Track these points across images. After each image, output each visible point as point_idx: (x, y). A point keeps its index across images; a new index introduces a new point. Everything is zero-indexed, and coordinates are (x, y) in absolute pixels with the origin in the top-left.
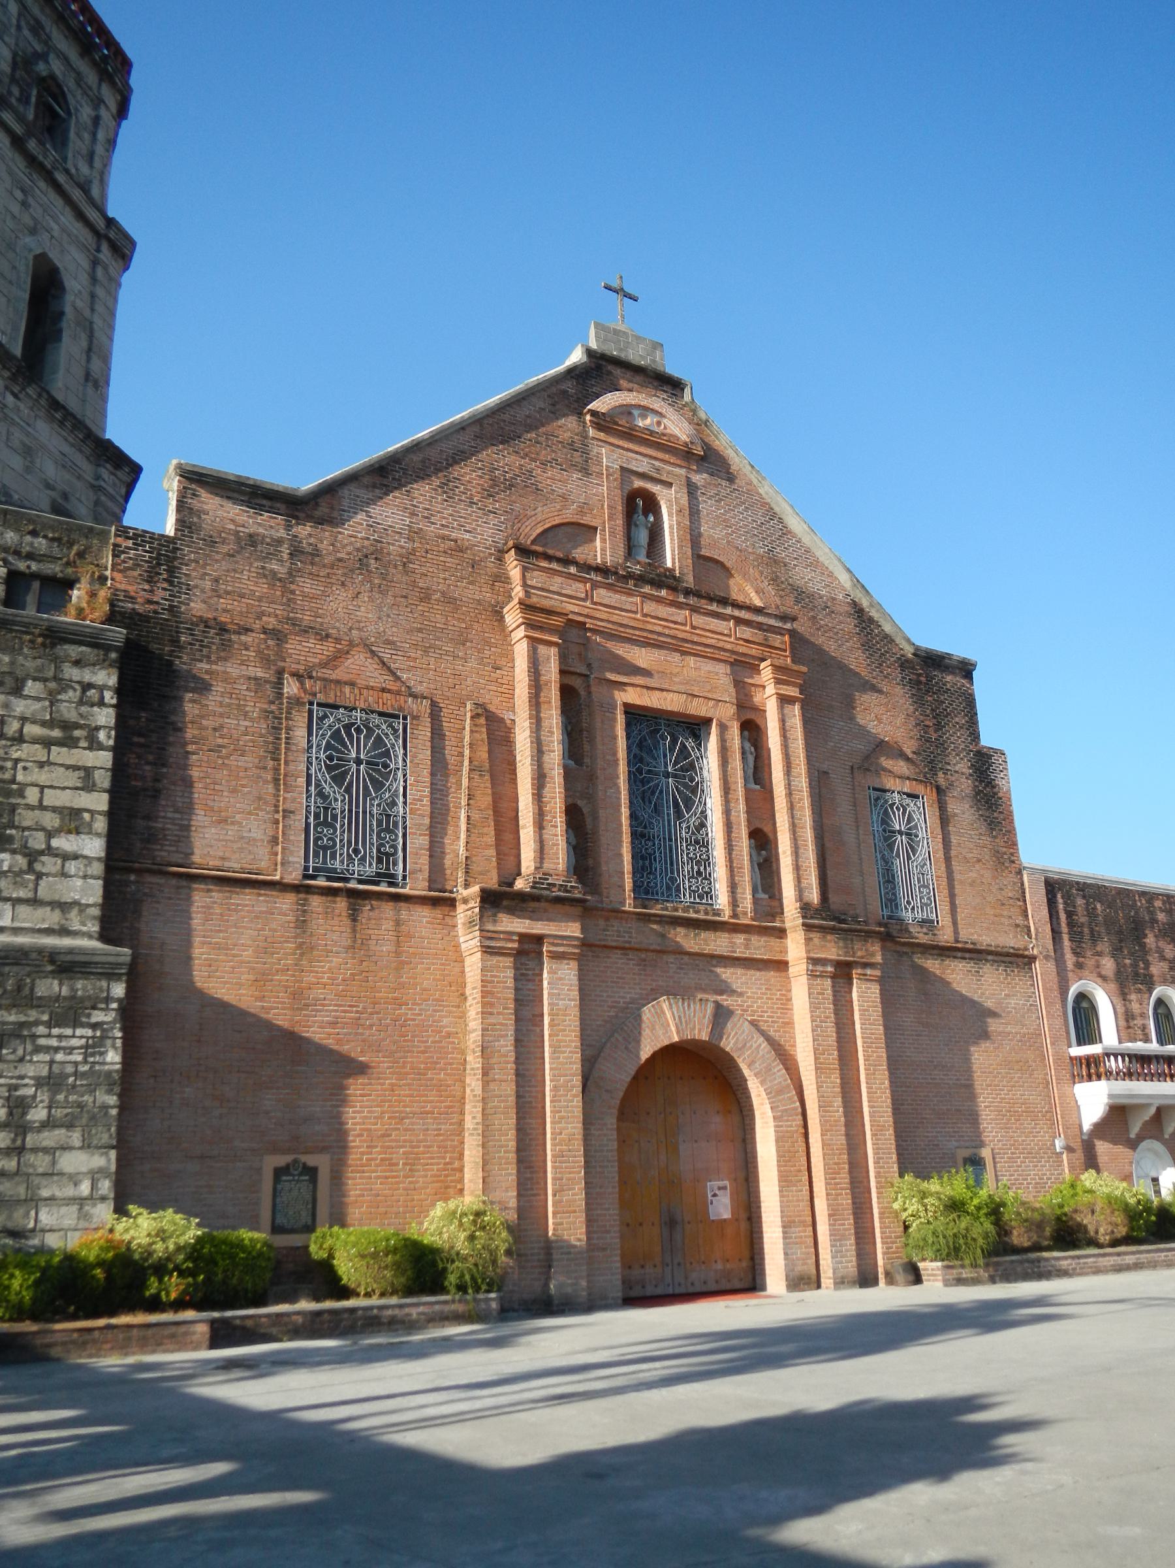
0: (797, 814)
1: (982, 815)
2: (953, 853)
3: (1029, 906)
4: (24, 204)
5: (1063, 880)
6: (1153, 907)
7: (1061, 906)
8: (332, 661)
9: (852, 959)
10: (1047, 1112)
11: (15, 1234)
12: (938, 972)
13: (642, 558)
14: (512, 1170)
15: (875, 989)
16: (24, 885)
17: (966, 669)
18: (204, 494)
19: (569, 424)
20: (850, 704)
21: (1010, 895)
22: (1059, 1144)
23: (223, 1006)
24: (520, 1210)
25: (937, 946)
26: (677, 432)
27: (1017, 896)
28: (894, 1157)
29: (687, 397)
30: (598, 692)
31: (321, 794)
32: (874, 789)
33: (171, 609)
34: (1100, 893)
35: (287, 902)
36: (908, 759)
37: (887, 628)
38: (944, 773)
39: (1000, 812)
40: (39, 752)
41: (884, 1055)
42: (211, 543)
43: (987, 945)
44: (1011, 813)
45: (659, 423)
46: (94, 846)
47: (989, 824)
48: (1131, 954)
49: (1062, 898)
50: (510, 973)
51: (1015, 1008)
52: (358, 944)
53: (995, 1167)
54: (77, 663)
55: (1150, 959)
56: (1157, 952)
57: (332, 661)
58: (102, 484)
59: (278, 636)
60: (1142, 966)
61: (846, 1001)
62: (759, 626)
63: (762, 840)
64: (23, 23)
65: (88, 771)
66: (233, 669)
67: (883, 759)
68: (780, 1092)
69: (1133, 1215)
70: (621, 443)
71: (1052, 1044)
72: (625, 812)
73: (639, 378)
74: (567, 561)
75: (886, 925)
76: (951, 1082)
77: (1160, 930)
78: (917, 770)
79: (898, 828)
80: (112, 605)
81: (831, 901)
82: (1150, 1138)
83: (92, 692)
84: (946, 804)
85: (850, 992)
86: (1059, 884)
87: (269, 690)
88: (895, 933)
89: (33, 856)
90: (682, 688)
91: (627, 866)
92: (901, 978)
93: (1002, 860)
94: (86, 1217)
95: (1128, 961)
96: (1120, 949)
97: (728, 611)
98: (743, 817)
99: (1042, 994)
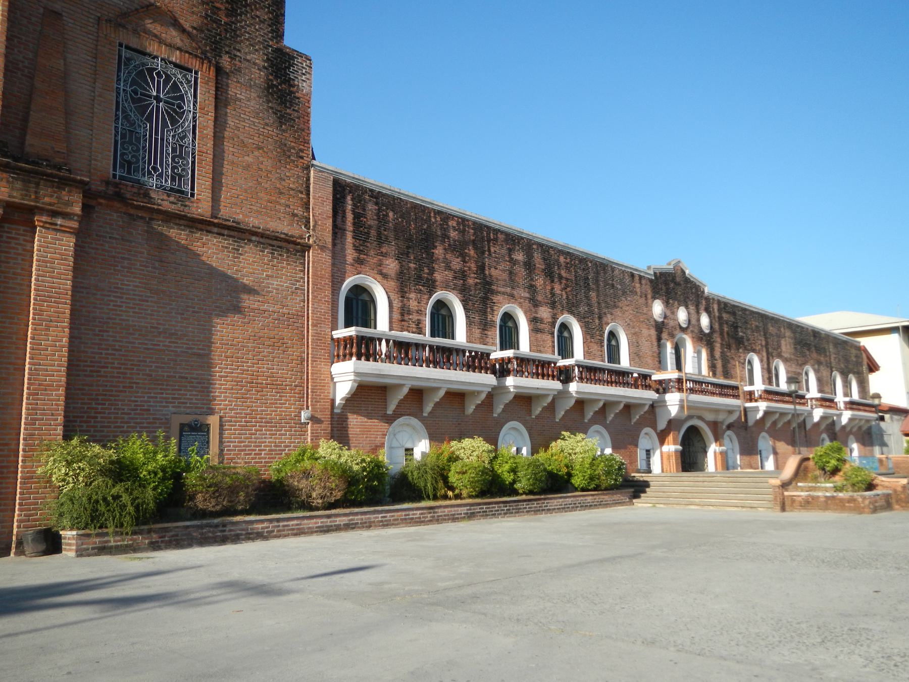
1: (272, 108)
2: (227, 134)
3: (311, 200)
5: (355, 185)
6: (447, 225)
7: (349, 207)
9: (32, 203)
10: (296, 386)
12: (183, 242)
15: (68, 243)
21: (291, 186)
22: (304, 415)
25: (185, 216)
27: (300, 188)
28: (60, 419)
32: (127, 47)
34: (394, 204)
36: (183, 31)
38: (229, 57)
39: (294, 110)
41: (68, 311)
43: (253, 227)
44: (308, 114)
47: (278, 118)
48: (417, 260)
49: (352, 199)
51: (277, 289)
53: (221, 434)
55: (436, 267)
56: (444, 262)
60: (426, 271)
61: (25, 250)
67: (148, 21)
69: (350, 480)
71: (313, 325)
75: (116, 185)
76: (178, 350)
77: (449, 245)
78: (194, 45)
79: (155, 94)
81: (27, 143)
82: (408, 415)
84: (228, 87)
85: (34, 243)
86: (351, 187)
88: (128, 196)
92: (131, 242)
93: (288, 153)
95: (412, 265)
96: (407, 254)
99: (310, 280)
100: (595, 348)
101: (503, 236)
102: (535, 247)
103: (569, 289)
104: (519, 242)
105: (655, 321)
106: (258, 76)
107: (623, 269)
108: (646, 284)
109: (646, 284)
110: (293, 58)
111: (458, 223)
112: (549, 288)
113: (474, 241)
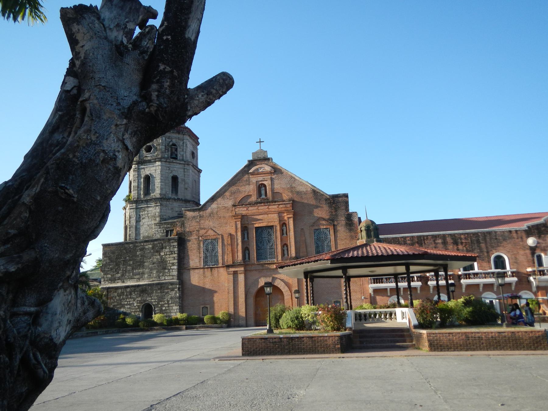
0: (291, 240)
4: (169, 170)
6: (406, 240)
8: (206, 233)
11: (169, 316)
13: (263, 197)
14: (233, 307)
16: (168, 274)
17: (346, 196)
18: (187, 212)
19: (246, 176)
20: (311, 212)
22: (363, 297)
23: (195, 286)
24: (234, 313)
26: (268, 169)
29: (271, 161)
30: (250, 226)
31: (205, 254)
33: (184, 231)
35: (202, 270)
37: (322, 193)
40: (168, 256)
42: (189, 219)
45: (264, 169)
46: (176, 267)
50: (232, 277)
52: (212, 275)
54: (172, 243)
57: (206, 233)
58: (187, 206)
59: (198, 231)
62: (284, 204)
63: (285, 246)
64: (166, 139)
65: (174, 257)
66: (193, 238)
68: (287, 291)
70: (256, 176)
72: (255, 246)
73: (260, 161)
74: (242, 205)
80: (177, 232)
83: (174, 246)
84: (337, 228)
87: (197, 240)
89: (169, 270)
90: (266, 221)
91: (255, 256)
94: (176, 314)
97: (277, 203)
98: (280, 242)
100: (485, 264)
101: (431, 237)
102: (447, 236)
103: (467, 246)
104: (438, 237)
105: (530, 247)
106: (343, 223)
107: (503, 230)
108: (521, 233)
109: (521, 233)
110: (352, 214)
111: (410, 238)
112: (456, 248)
113: (417, 242)
